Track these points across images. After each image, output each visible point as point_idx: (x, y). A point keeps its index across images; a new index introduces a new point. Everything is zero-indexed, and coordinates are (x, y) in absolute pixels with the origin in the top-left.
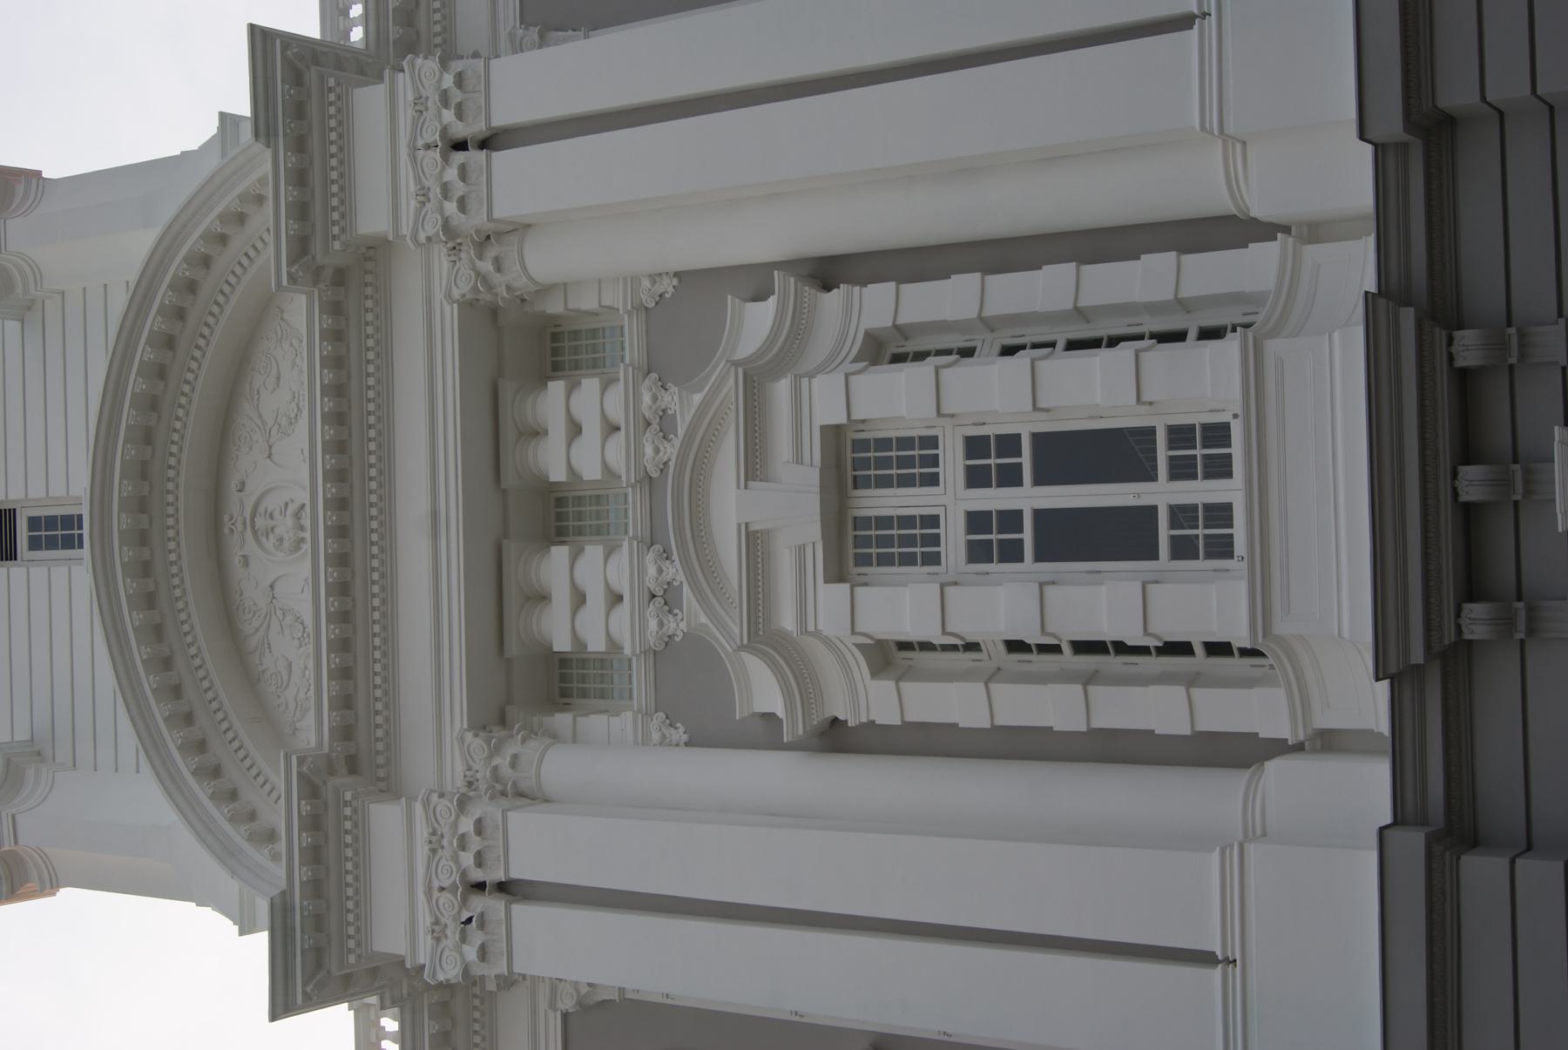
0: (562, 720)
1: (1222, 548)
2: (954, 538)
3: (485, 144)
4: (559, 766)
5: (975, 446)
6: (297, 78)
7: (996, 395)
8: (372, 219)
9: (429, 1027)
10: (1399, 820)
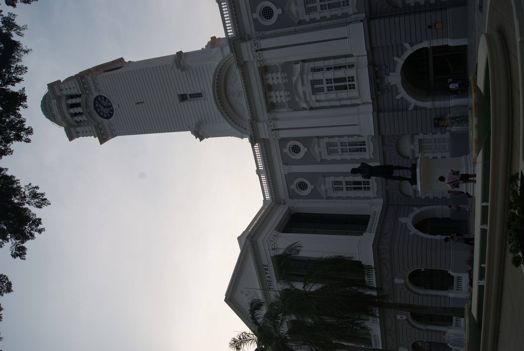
0: (277, 110)
1: (354, 88)
2: (326, 89)
3: (260, 50)
5: (327, 80)
6: (234, 44)
7: (330, 75)
8: (246, 59)
9: (263, 144)
10: (373, 111)
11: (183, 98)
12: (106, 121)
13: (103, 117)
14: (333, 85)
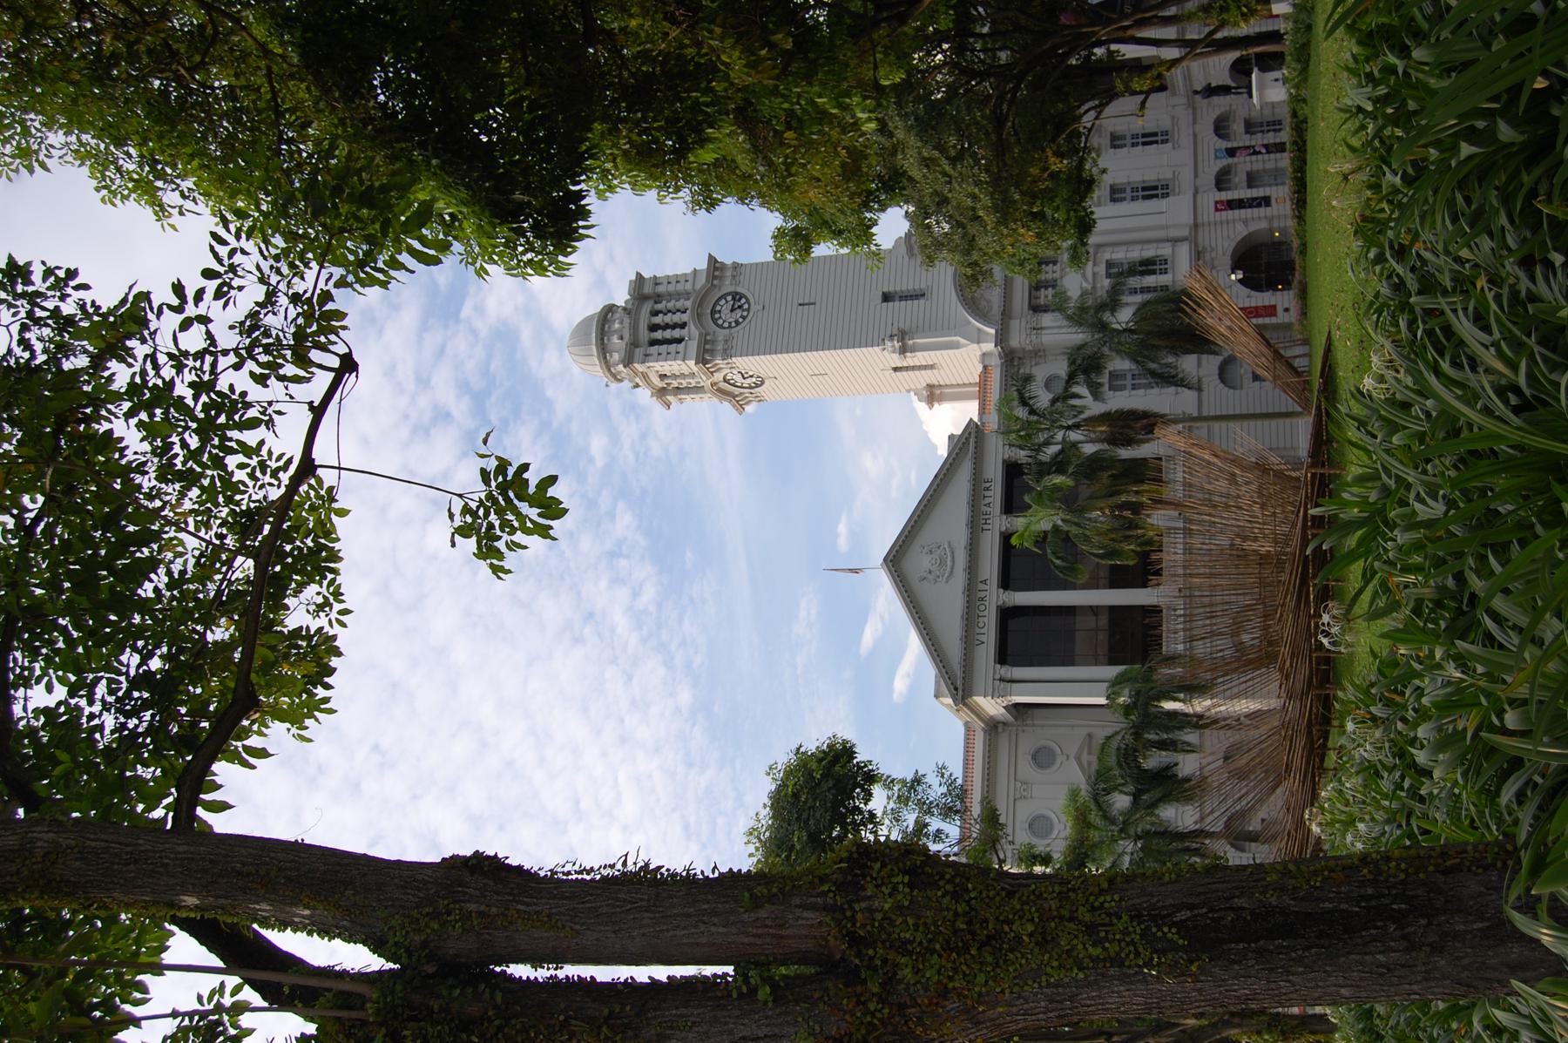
11: (887, 298)
12: (721, 334)
13: (721, 327)
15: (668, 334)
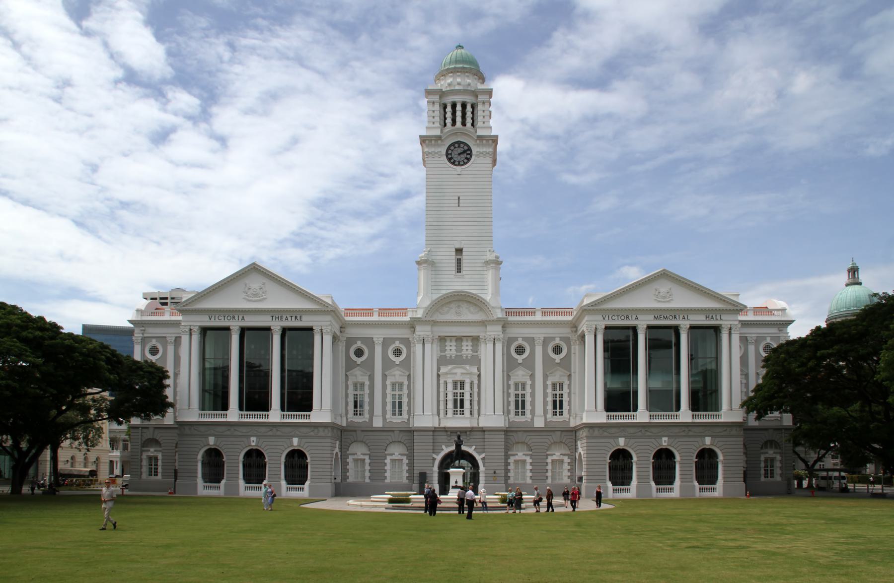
4: (435, 346)
7: (467, 398)
8: (489, 328)
11: (459, 251)
12: (443, 150)
14: (459, 398)
15: (449, 115)
